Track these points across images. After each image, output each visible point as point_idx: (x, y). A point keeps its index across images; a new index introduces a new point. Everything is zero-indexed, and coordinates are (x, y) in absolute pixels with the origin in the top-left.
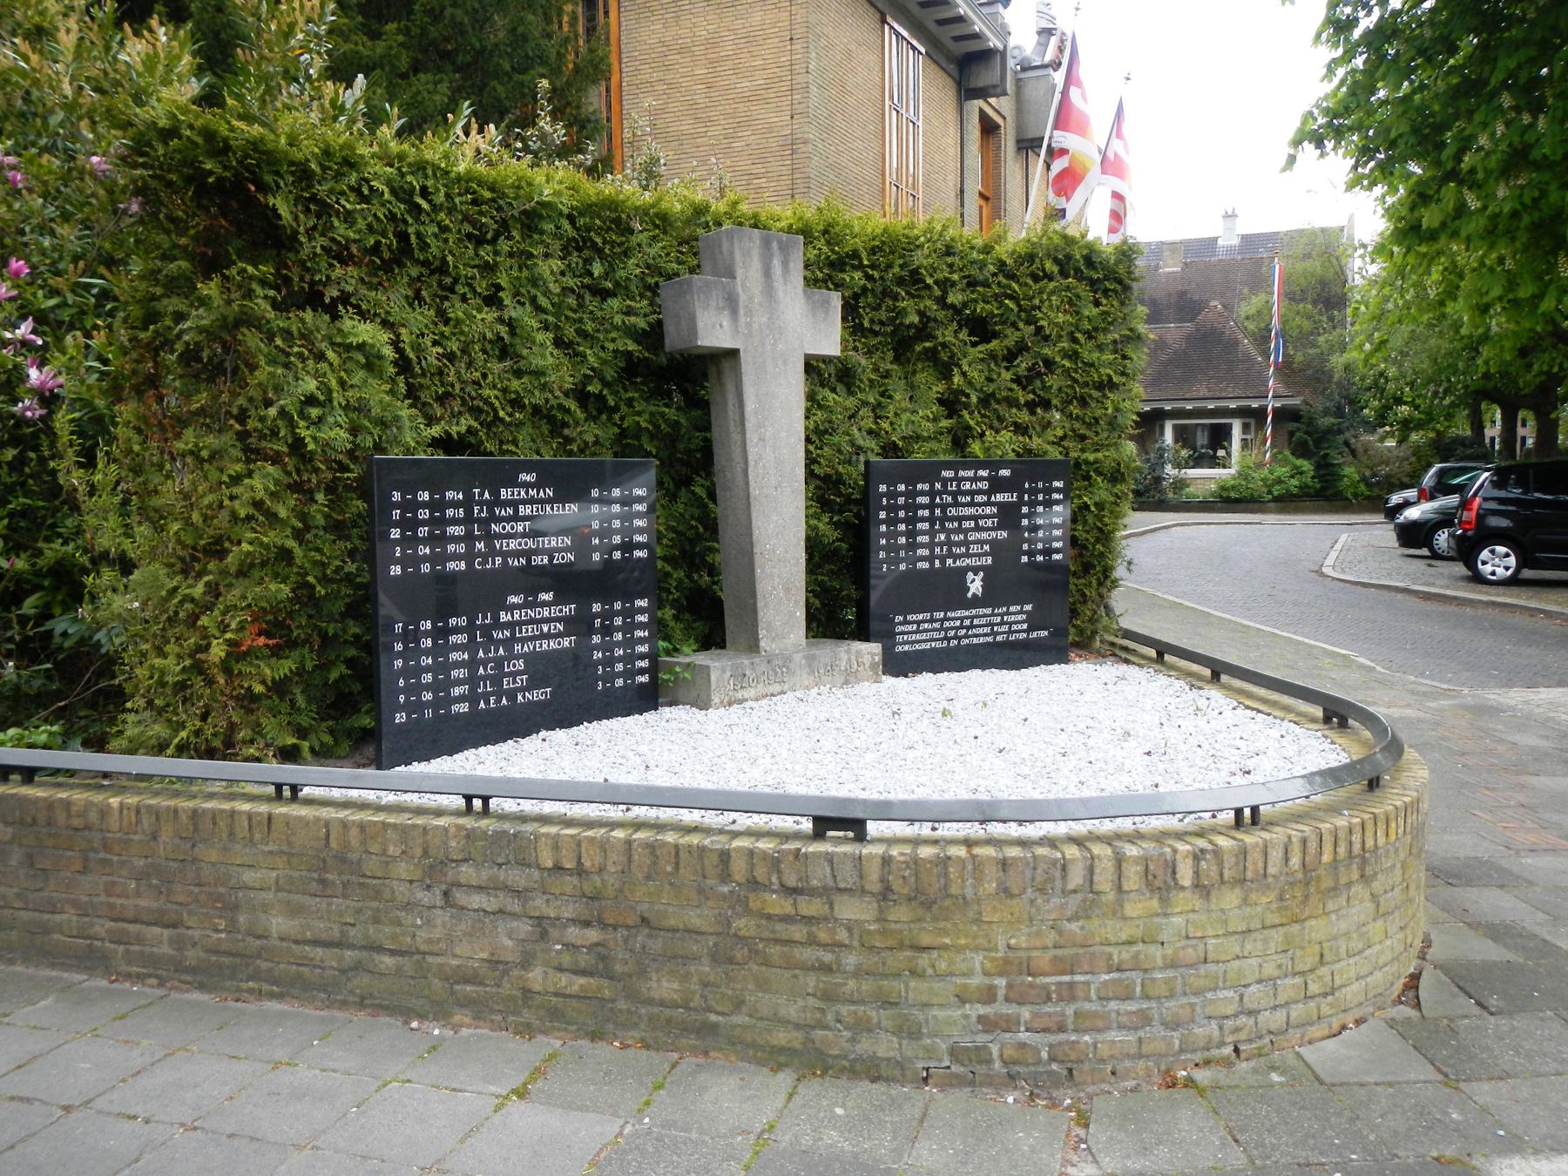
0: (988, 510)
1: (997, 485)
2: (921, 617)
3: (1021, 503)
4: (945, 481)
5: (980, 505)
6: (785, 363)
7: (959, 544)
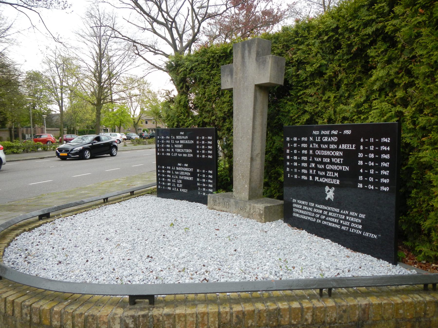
0: (337, 153)
1: (342, 139)
2: (303, 203)
3: (358, 150)
4: (314, 136)
5: (332, 150)
6: (247, 90)
7: (322, 170)
